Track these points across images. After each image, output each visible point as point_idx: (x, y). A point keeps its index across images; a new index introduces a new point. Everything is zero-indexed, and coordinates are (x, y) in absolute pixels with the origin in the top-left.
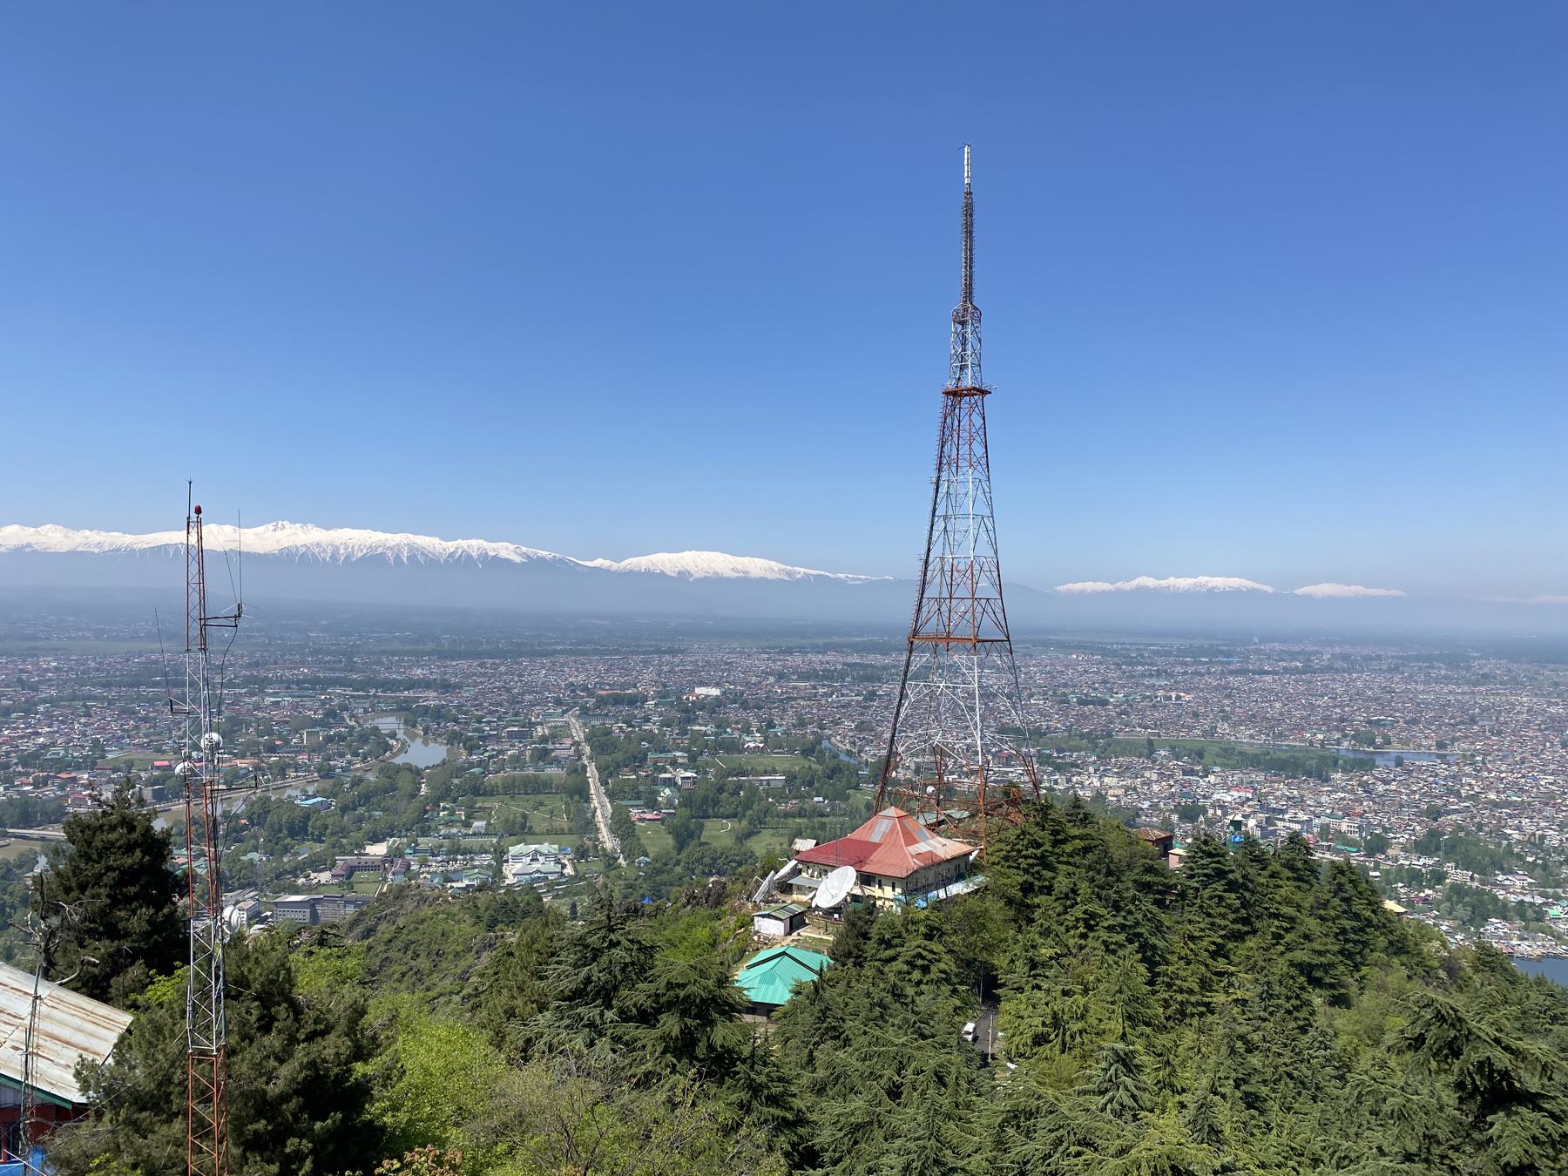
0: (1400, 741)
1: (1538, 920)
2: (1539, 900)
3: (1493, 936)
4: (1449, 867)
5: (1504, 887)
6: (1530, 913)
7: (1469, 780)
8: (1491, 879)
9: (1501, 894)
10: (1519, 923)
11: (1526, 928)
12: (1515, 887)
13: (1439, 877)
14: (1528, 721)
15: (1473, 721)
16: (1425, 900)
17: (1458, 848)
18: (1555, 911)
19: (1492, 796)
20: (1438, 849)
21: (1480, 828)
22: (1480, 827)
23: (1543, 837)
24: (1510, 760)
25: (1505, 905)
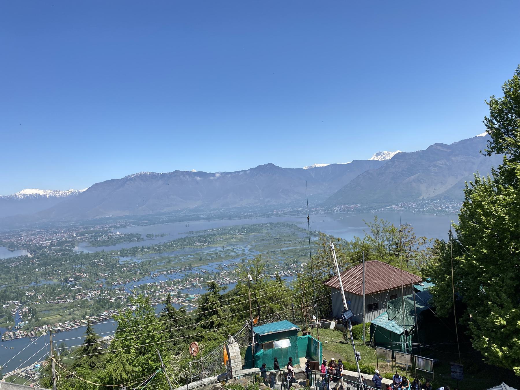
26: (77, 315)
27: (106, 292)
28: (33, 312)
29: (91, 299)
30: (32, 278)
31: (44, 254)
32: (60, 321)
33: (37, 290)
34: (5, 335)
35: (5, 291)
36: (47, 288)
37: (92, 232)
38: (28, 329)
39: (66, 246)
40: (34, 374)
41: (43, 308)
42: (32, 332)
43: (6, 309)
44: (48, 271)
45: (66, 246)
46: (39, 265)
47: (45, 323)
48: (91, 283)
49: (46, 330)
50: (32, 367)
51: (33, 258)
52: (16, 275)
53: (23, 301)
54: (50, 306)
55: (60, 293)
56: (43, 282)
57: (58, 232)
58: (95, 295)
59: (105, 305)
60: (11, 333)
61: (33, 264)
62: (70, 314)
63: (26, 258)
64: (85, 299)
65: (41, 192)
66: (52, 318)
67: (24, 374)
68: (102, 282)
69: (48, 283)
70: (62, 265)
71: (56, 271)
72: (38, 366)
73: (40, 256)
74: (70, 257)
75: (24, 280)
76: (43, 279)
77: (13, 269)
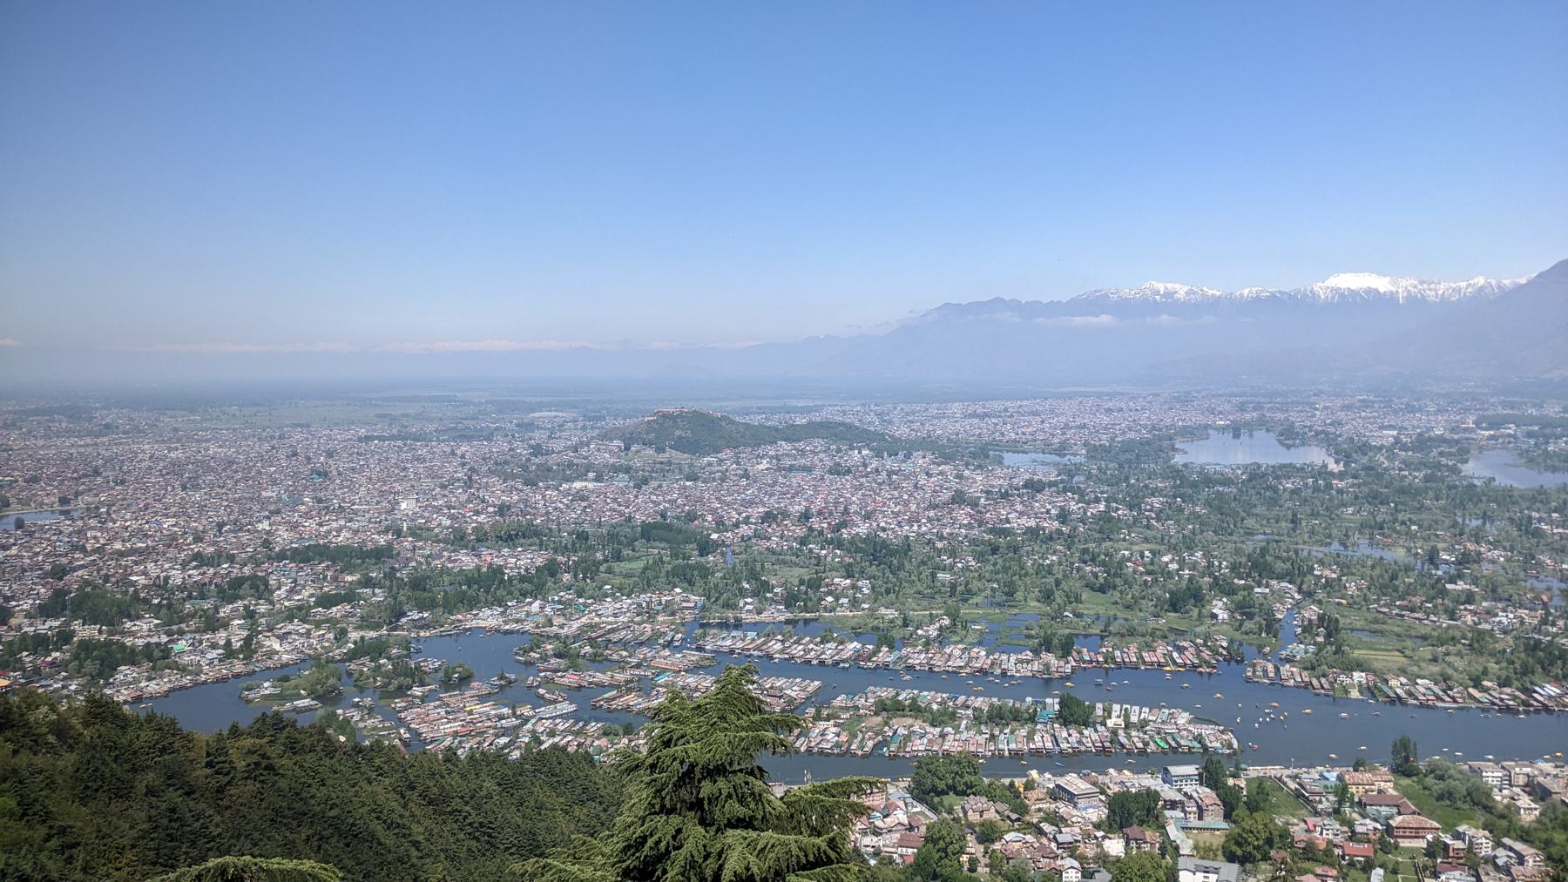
0: (20, 501)
1: (164, 658)
2: (164, 639)
3: (123, 683)
4: (76, 625)
5: (133, 634)
6: (157, 653)
7: (94, 533)
8: (119, 629)
9: (128, 641)
10: (147, 665)
11: (153, 668)
12: (142, 631)
13: (65, 637)
14: (150, 468)
15: (97, 472)
16: (52, 664)
17: (88, 605)
18: (182, 645)
19: (118, 546)
20: (64, 609)
21: (106, 578)
22: (106, 578)
23: (167, 578)
24: (134, 508)
25: (133, 650)
26: (1456, 670)
27: (1561, 623)
28: (1329, 625)
29: (1505, 633)
30: (1335, 532)
31: (1373, 469)
32: (1403, 671)
33: (1346, 568)
34: (1254, 666)
35: (1264, 551)
36: (1373, 567)
37: (1532, 420)
38: (1313, 669)
39: (1441, 454)
40: (1320, 794)
41: (1354, 619)
42: (1323, 680)
43: (1262, 600)
44: (1379, 519)
45: (1441, 454)
46: (1356, 498)
47: (1360, 666)
48: (1511, 582)
49: (1360, 685)
50: (1314, 774)
51: (1341, 476)
52: (1294, 515)
53: (1304, 587)
54: (1376, 621)
55: (1410, 591)
56: (1363, 548)
57: (1420, 410)
58: (1522, 622)
59: (1552, 664)
60: (1270, 667)
61: (1340, 491)
62: (1435, 660)
63: (1323, 472)
64: (1488, 627)
65: (1382, 284)
66: (1381, 655)
67: (1293, 786)
68: (1549, 589)
69: (1377, 554)
70: (1421, 508)
71: (1403, 523)
72: (1332, 776)
73: (1362, 473)
74: (1449, 488)
75: (1312, 532)
76: (1364, 541)
77: (1286, 496)
